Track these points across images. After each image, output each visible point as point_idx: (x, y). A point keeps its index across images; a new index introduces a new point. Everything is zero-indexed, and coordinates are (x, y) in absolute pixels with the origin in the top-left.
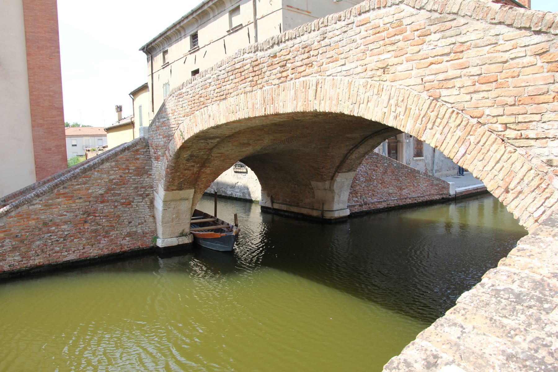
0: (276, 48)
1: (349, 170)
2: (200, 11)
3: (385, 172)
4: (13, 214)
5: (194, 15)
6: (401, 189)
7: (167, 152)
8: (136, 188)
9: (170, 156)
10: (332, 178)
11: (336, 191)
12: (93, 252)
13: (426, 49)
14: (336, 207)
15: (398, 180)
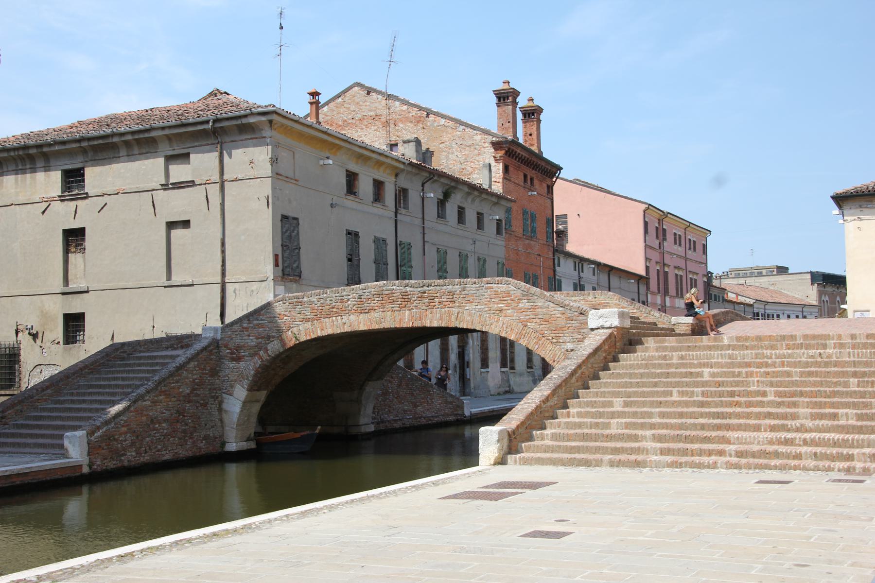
0: (425, 288)
1: (378, 379)
2: (101, 142)
3: (399, 386)
4: (132, 409)
5: (84, 144)
7: (261, 353)
8: (210, 389)
10: (361, 388)
11: (363, 402)
12: (183, 453)
13: (521, 305)
14: (362, 421)
15: (413, 395)
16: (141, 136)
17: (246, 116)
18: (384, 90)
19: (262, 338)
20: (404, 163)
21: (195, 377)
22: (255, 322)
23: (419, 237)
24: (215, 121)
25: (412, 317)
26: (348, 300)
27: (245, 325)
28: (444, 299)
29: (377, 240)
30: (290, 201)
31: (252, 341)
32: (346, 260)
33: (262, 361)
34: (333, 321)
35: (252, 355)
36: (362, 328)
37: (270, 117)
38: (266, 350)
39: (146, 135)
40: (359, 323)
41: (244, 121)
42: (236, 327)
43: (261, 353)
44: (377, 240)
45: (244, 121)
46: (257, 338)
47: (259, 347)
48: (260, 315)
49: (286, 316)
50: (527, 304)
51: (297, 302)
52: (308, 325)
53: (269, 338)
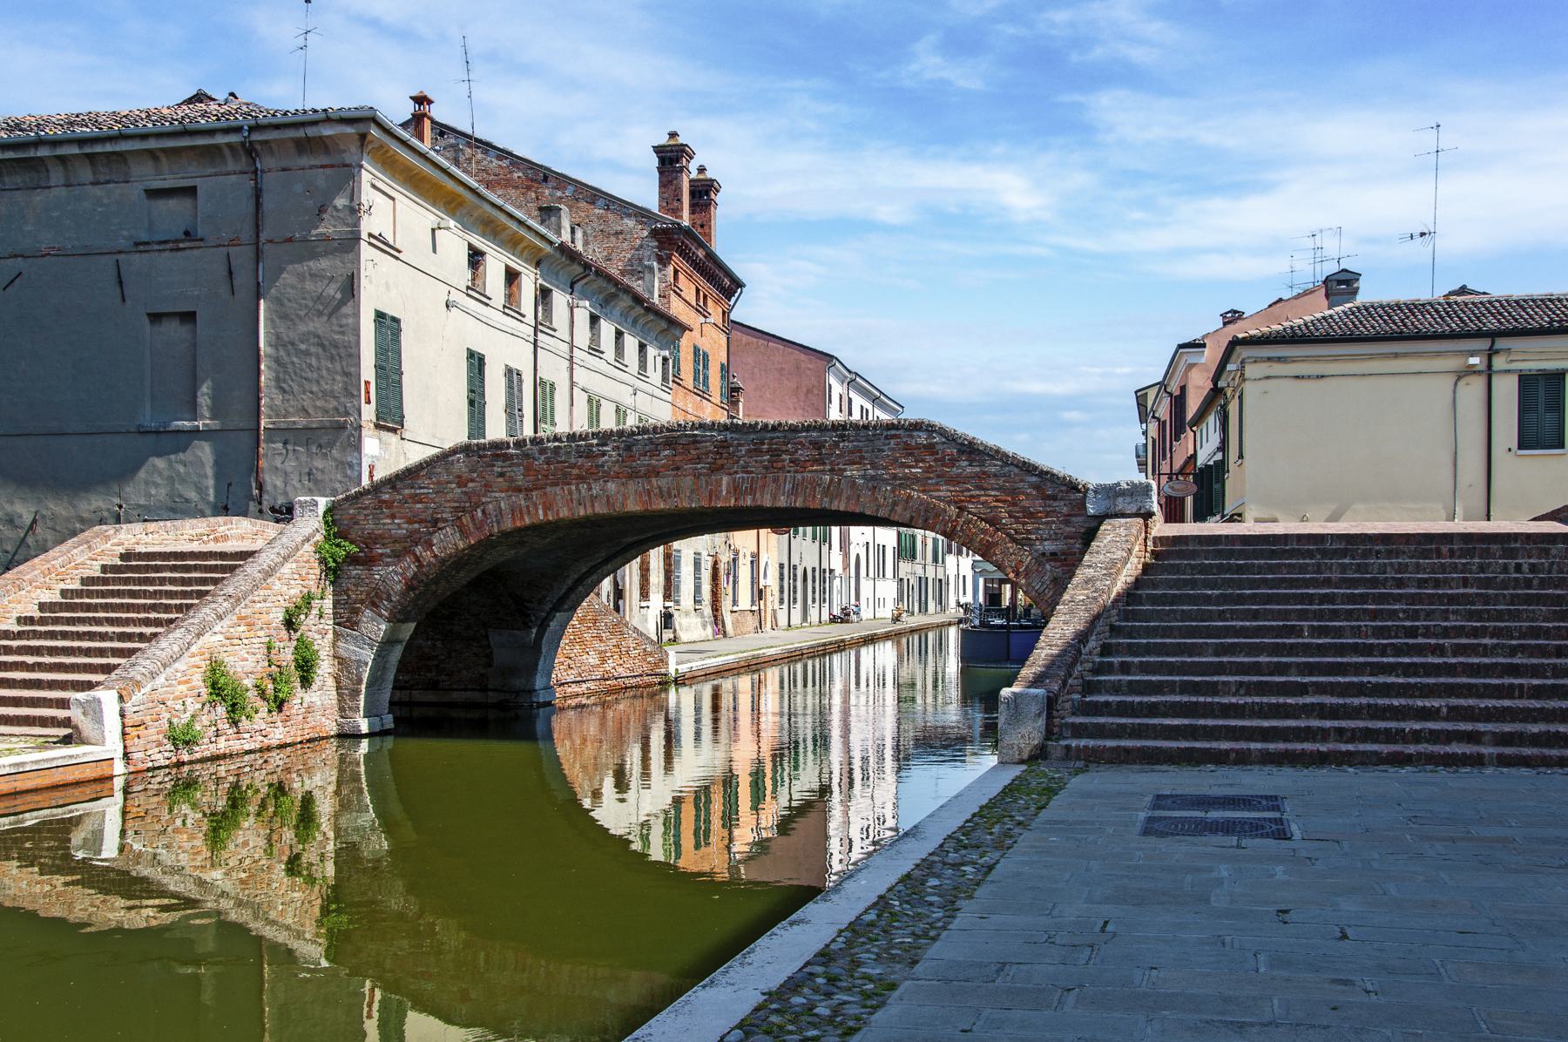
4: (193, 649)
6: (603, 661)
7: (418, 550)
9: (435, 556)
16: (98, 149)
17: (314, 123)
18: (469, 132)
20: (551, 243)
21: (292, 592)
22: (407, 491)
23: (567, 375)
24: (252, 129)
25: (736, 489)
26: (604, 454)
27: (386, 497)
28: (802, 454)
29: (509, 372)
30: (387, 286)
31: (399, 527)
32: (466, 402)
33: (420, 566)
34: (570, 493)
35: (398, 556)
36: (633, 506)
37: (361, 128)
38: (430, 545)
39: (109, 148)
40: (625, 497)
41: (311, 132)
43: (418, 550)
44: (509, 372)
45: (311, 132)
46: (410, 522)
47: (413, 539)
48: (418, 477)
49: (472, 480)
50: (969, 470)
53: (435, 522)
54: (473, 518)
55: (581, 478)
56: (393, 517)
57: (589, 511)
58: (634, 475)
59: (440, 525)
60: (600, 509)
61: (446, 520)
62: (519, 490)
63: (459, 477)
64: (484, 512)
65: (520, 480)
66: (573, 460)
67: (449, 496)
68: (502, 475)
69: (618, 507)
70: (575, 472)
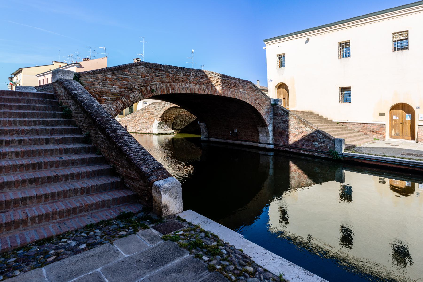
7: (124, 99)
19: (125, 88)
22: (119, 76)
27: (109, 76)
31: (115, 89)
35: (113, 100)
36: (197, 92)
42: (100, 76)
43: (124, 99)
46: (120, 88)
47: (121, 94)
49: (147, 76)
51: (157, 69)
52: (164, 86)
54: (146, 89)
55: (183, 82)
56: (113, 85)
57: (185, 92)
58: (197, 83)
59: (133, 90)
60: (188, 92)
61: (135, 89)
62: (163, 82)
63: (142, 74)
64: (150, 88)
65: (164, 79)
66: (181, 76)
67: (138, 81)
68: (158, 76)
69: (193, 92)
70: (182, 79)
